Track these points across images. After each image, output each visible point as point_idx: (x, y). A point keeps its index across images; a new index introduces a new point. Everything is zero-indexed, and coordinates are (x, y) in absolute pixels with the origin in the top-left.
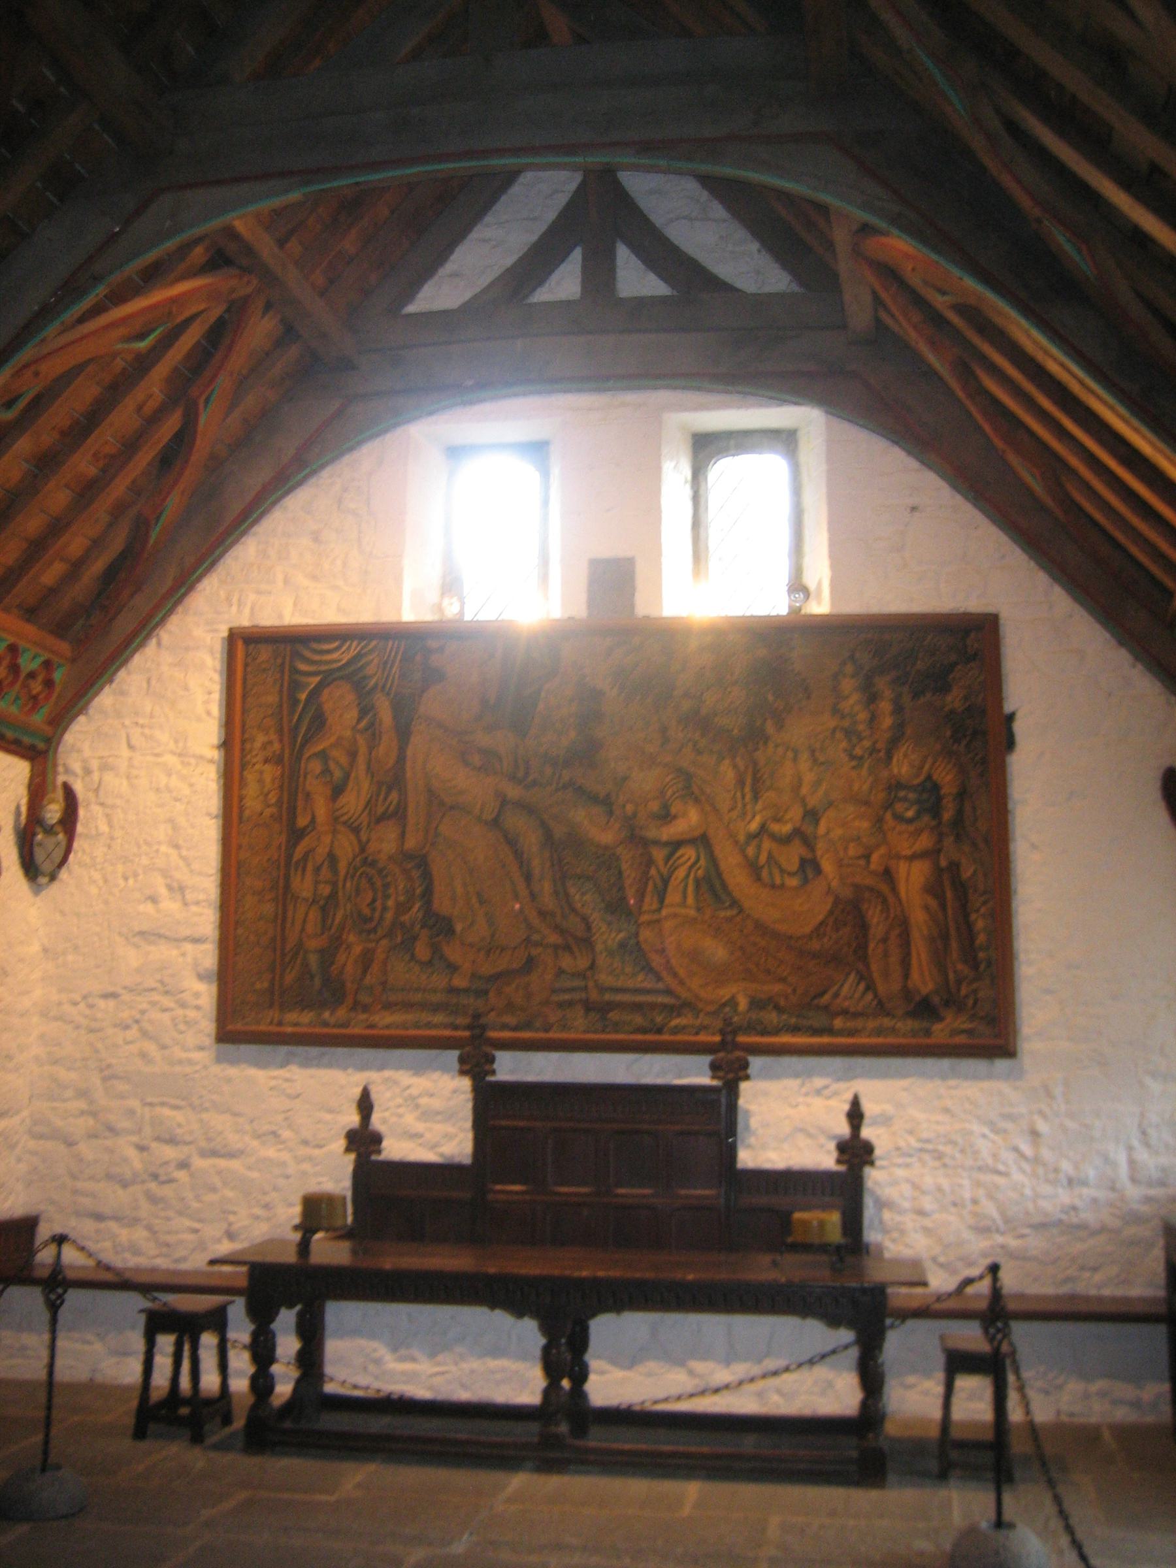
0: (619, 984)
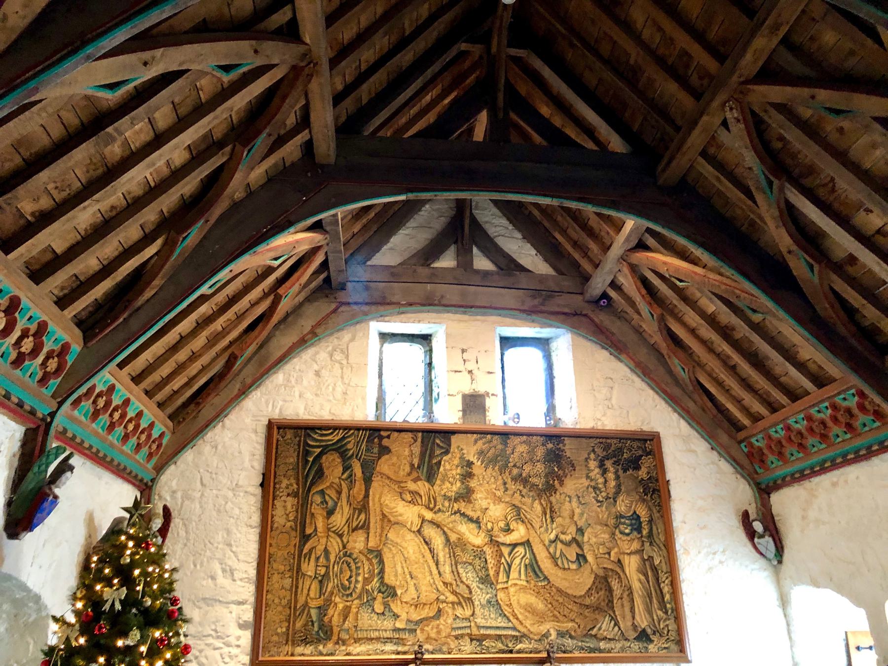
0: (488, 625)
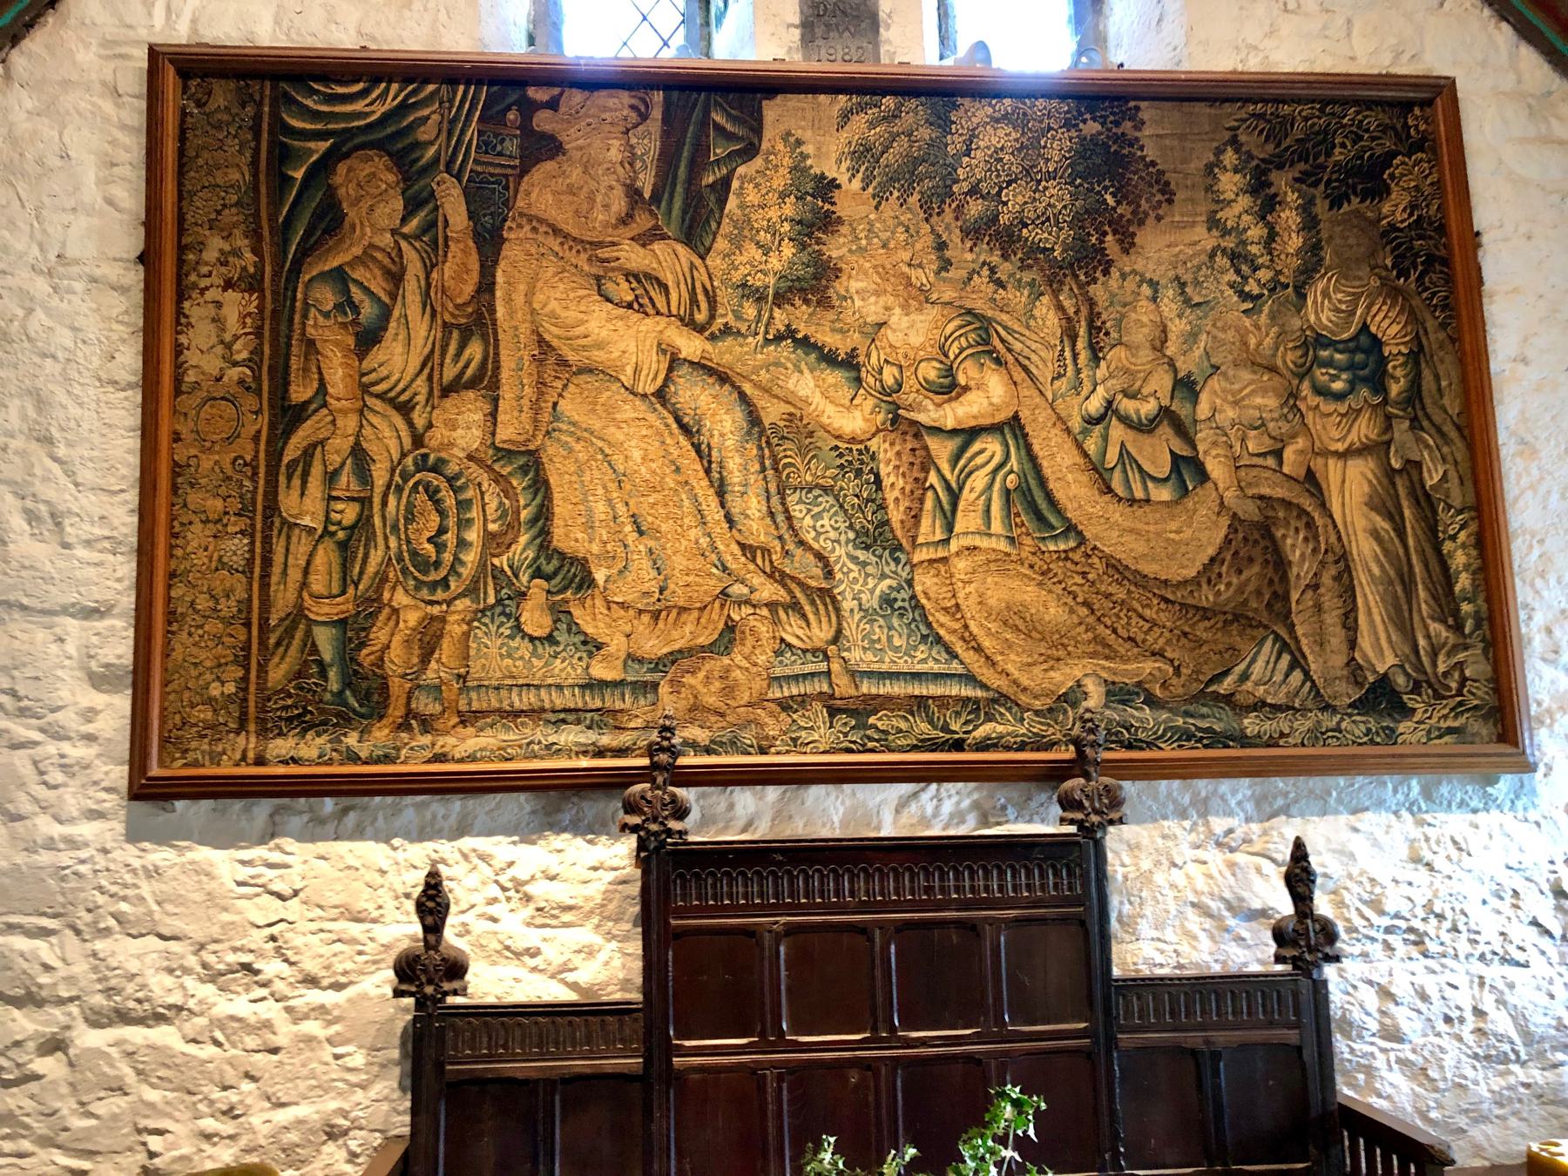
0: (884, 667)
